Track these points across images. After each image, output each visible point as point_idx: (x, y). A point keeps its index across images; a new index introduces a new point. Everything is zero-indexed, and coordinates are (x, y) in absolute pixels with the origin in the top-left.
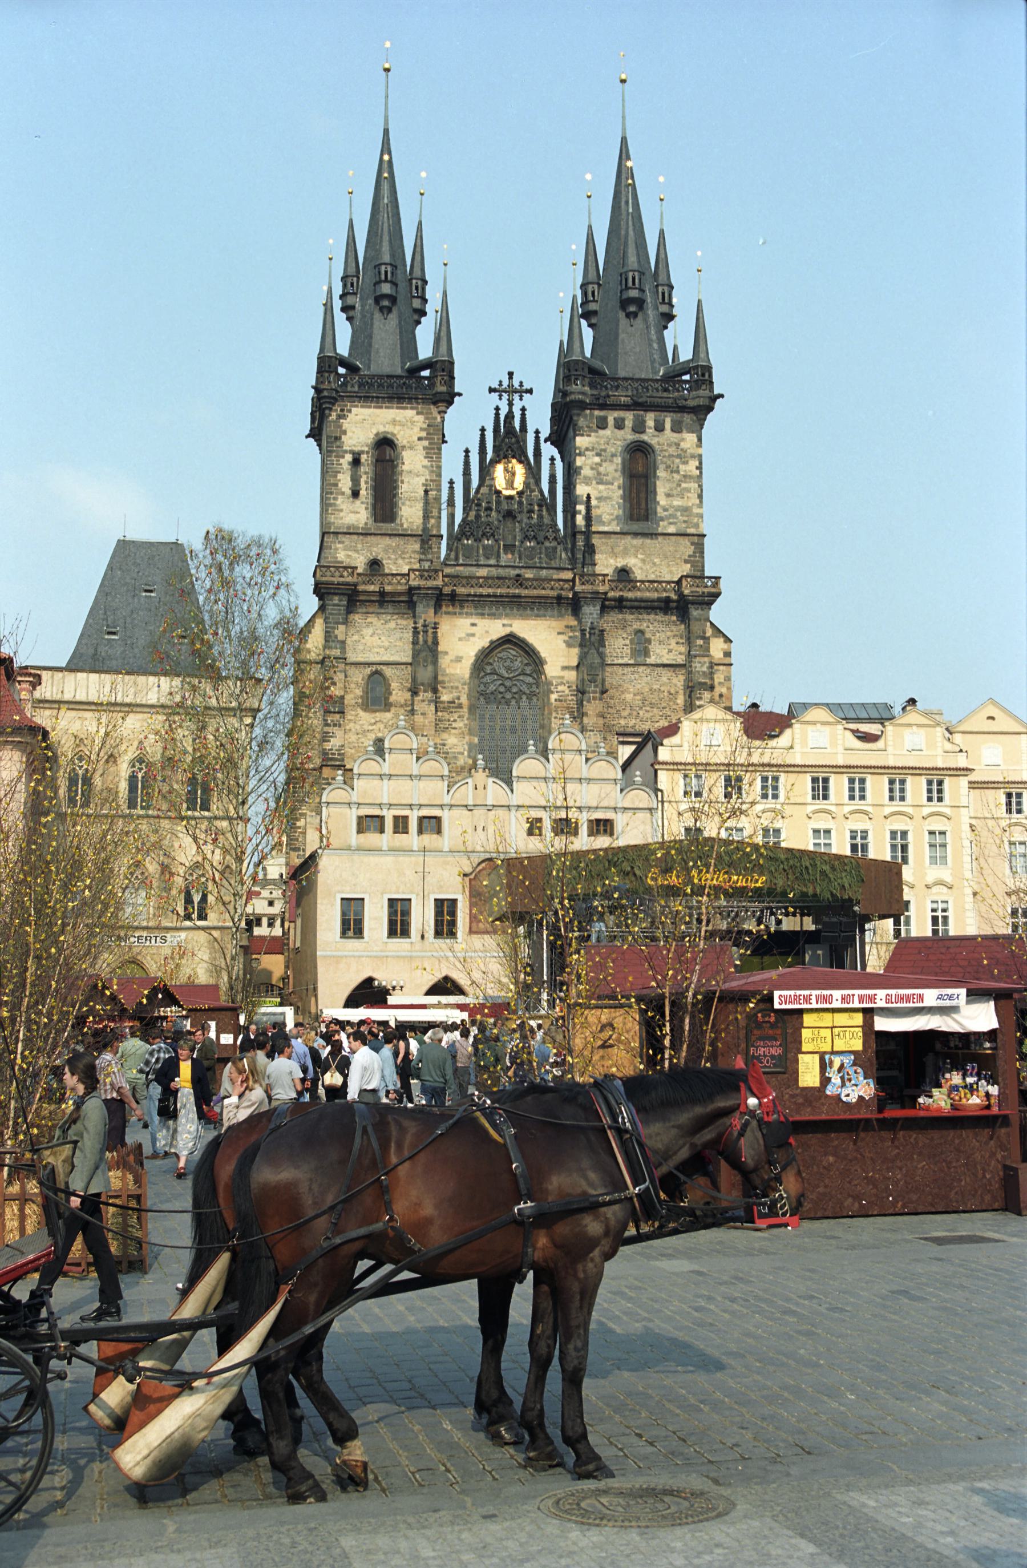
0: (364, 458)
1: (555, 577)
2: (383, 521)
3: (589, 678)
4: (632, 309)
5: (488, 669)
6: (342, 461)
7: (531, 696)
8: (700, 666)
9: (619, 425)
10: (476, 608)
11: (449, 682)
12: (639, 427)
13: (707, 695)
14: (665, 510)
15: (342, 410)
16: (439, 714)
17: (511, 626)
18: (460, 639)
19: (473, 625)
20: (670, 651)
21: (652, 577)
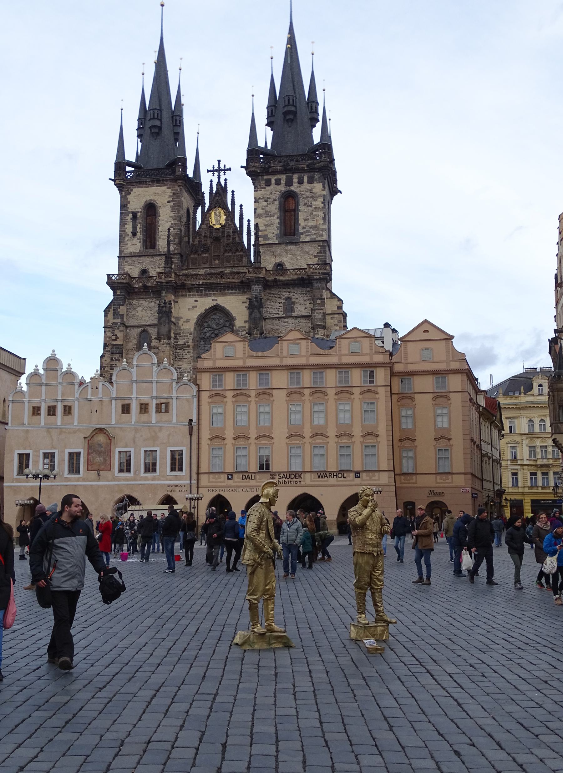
0: (139, 214)
1: (242, 271)
2: (151, 248)
3: (253, 326)
4: (291, 117)
5: (206, 325)
6: (127, 218)
8: (318, 315)
9: (278, 182)
10: (197, 291)
11: (183, 333)
13: (321, 332)
14: (304, 228)
15: (127, 190)
16: (178, 351)
17: (216, 300)
18: (189, 309)
19: (196, 301)
21: (295, 267)
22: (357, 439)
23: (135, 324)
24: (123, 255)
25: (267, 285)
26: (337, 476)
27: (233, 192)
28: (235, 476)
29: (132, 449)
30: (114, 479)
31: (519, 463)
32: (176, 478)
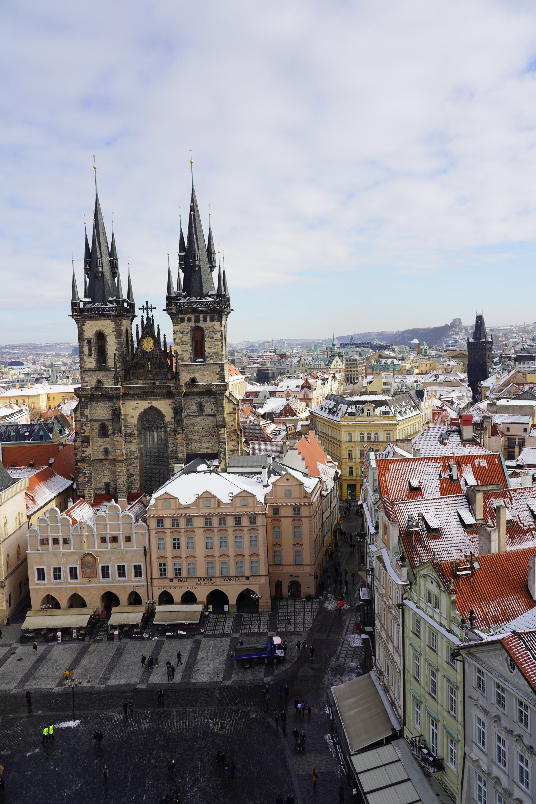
0: (92, 340)
5: (145, 419)
6: (84, 342)
7: (161, 429)
9: (189, 320)
12: (197, 320)
13: (223, 429)
14: (209, 354)
20: (212, 409)
22: (247, 557)
23: (96, 418)
24: (83, 369)
25: (186, 394)
26: (235, 579)
27: (158, 325)
28: (174, 580)
29: (109, 565)
30: (100, 582)
31: (354, 461)
32: (138, 581)
